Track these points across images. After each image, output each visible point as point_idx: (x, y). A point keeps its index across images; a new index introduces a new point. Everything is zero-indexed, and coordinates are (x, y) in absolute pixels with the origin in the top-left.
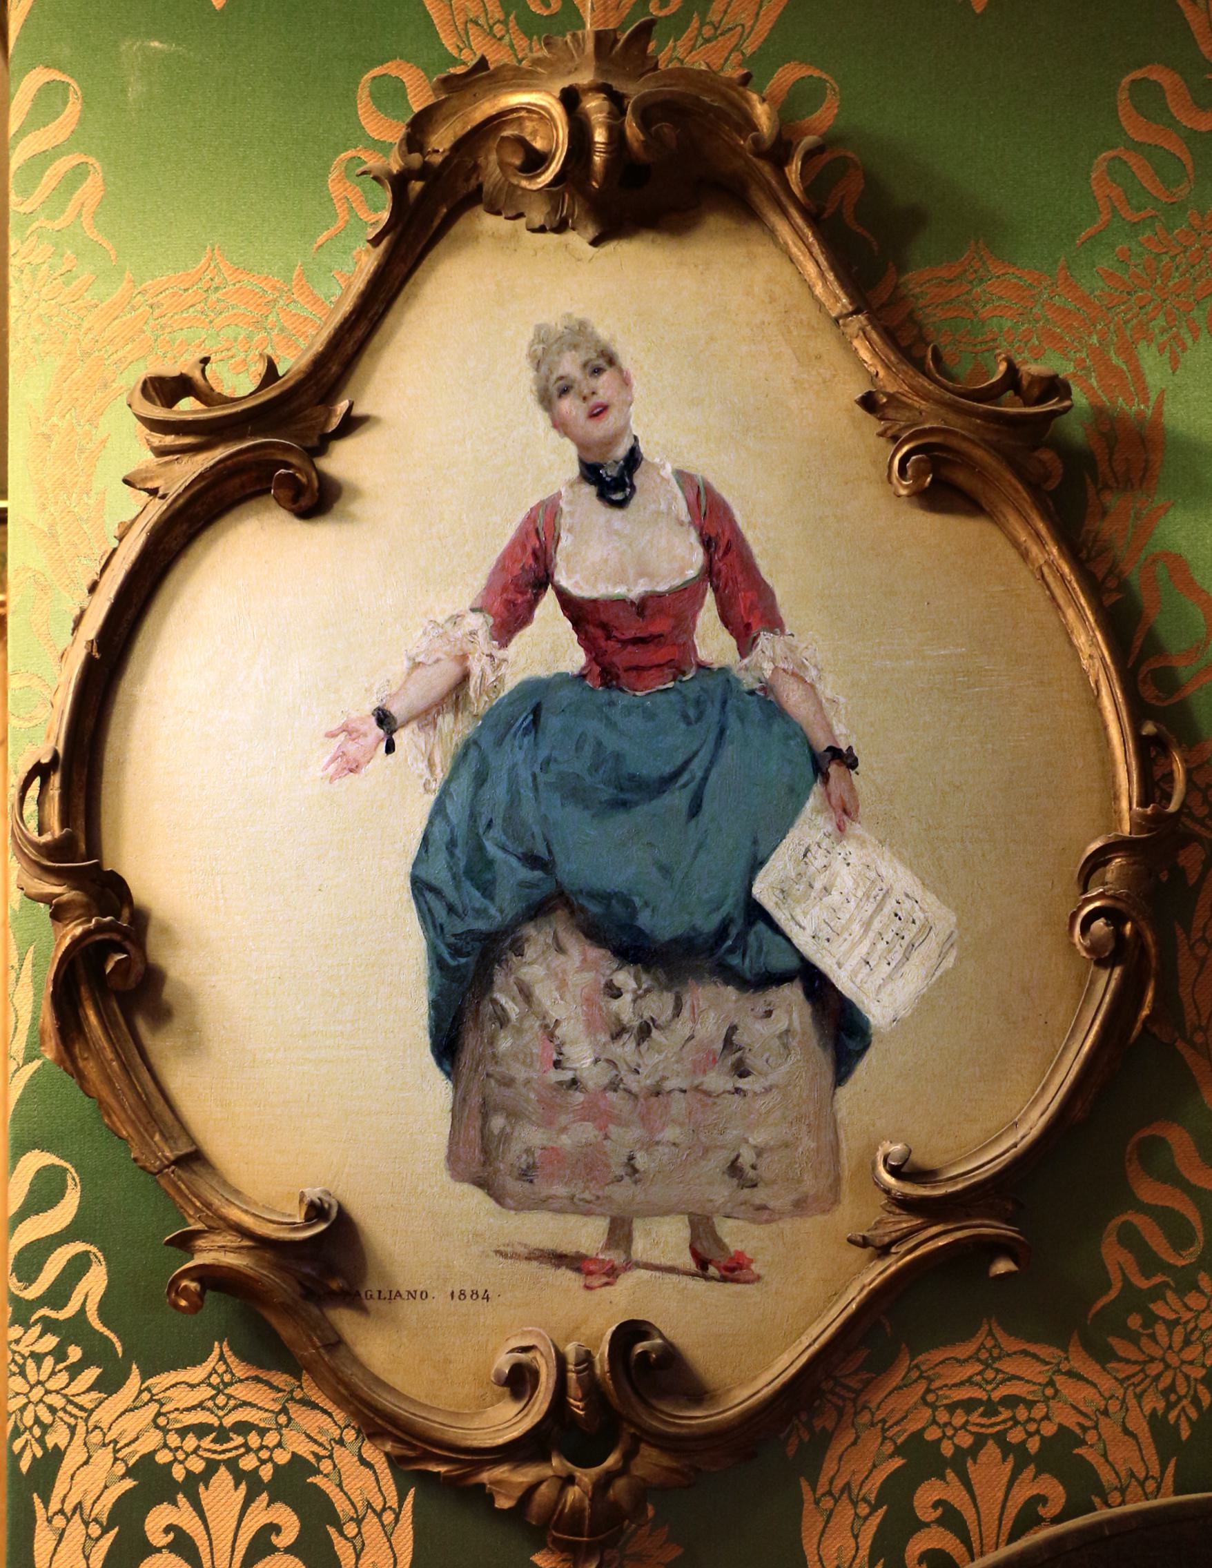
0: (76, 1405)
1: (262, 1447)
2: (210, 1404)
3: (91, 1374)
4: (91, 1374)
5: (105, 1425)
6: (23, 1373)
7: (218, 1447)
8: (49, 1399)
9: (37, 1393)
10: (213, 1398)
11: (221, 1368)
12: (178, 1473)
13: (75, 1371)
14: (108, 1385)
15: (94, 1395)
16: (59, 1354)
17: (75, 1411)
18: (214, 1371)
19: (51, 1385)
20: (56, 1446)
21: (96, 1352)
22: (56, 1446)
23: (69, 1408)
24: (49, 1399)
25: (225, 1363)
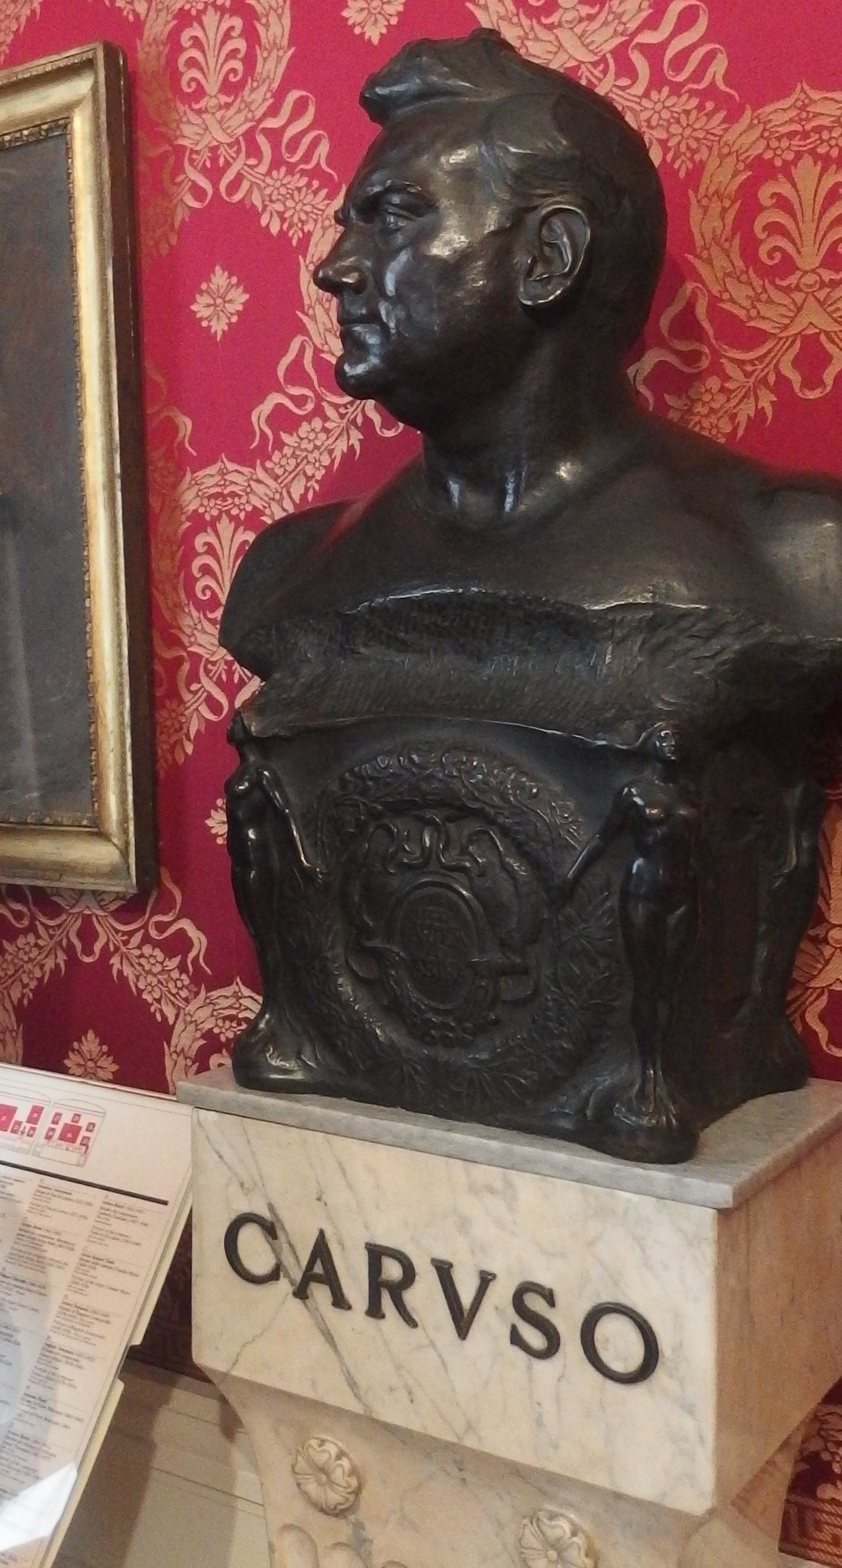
0: (713, 134)
1: (831, 138)
2: (797, 118)
3: (722, 115)
4: (722, 115)
5: (731, 142)
6: (678, 122)
7: (802, 143)
8: (695, 134)
9: (688, 132)
10: (798, 115)
11: (803, 96)
12: (778, 163)
13: (710, 116)
14: (732, 118)
15: (725, 126)
16: (700, 107)
17: (712, 138)
18: (798, 99)
19: (697, 126)
20: (701, 161)
21: (722, 100)
22: (701, 161)
23: (709, 136)
24: (695, 134)
25: (805, 93)
